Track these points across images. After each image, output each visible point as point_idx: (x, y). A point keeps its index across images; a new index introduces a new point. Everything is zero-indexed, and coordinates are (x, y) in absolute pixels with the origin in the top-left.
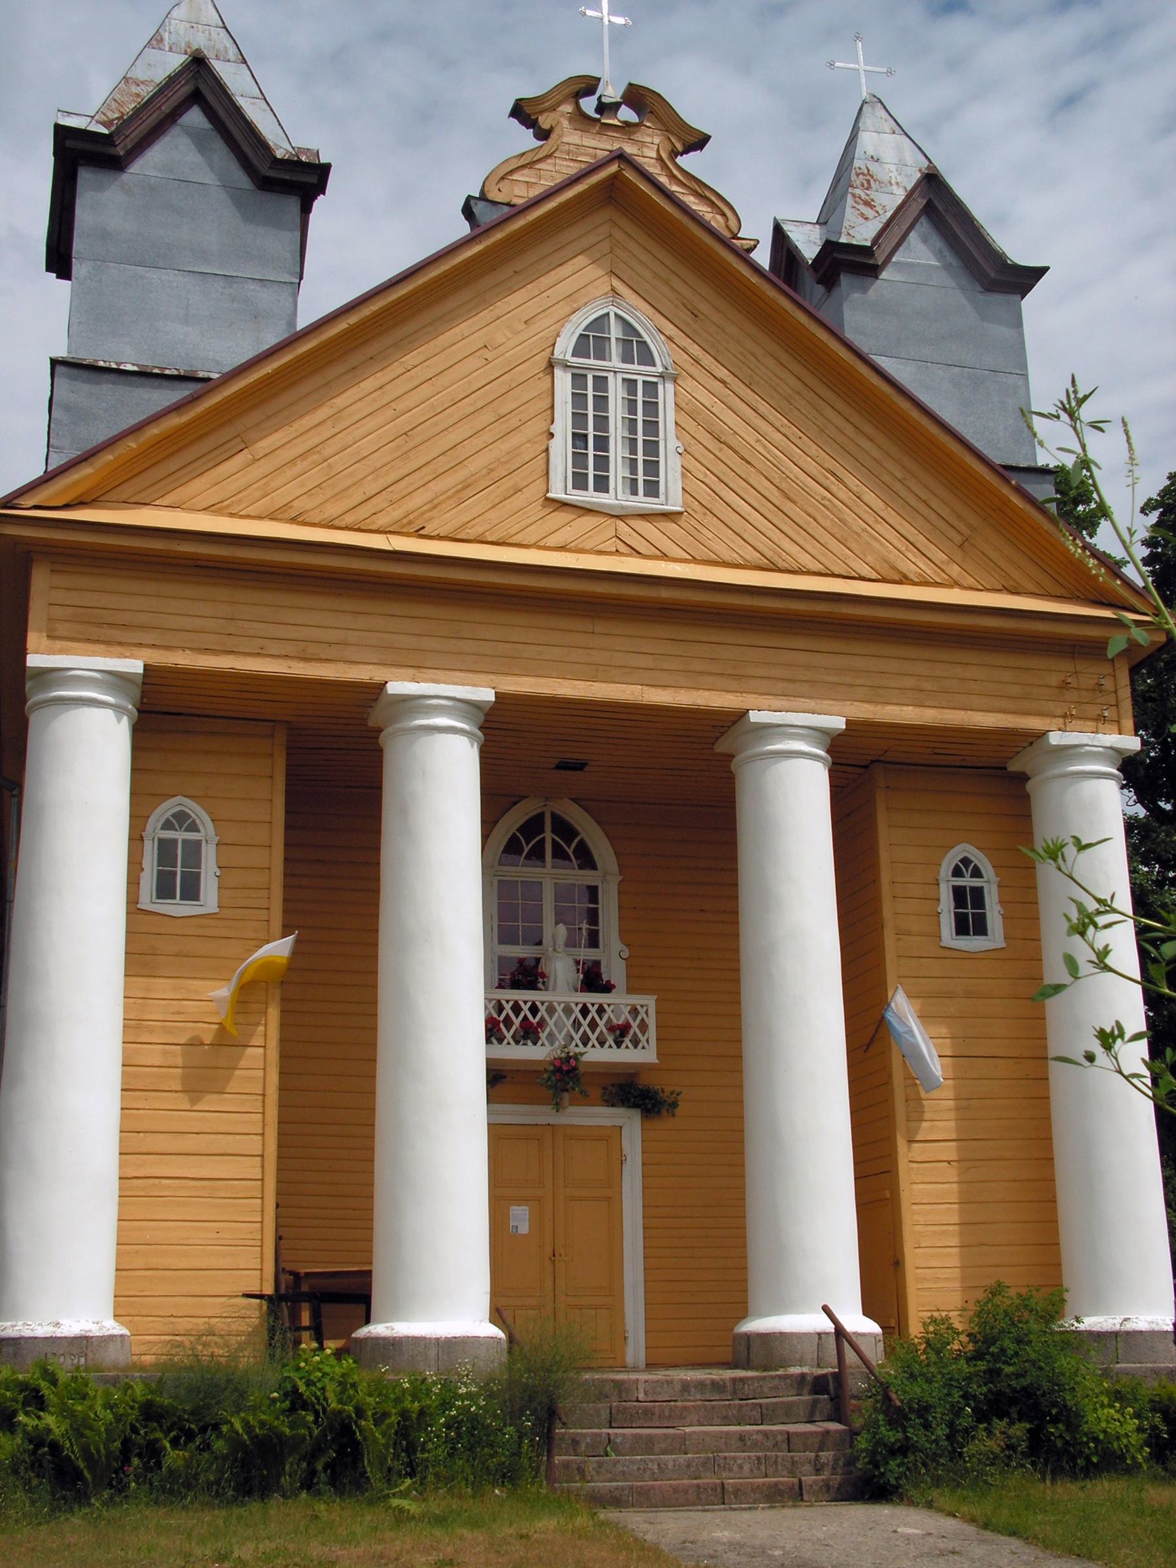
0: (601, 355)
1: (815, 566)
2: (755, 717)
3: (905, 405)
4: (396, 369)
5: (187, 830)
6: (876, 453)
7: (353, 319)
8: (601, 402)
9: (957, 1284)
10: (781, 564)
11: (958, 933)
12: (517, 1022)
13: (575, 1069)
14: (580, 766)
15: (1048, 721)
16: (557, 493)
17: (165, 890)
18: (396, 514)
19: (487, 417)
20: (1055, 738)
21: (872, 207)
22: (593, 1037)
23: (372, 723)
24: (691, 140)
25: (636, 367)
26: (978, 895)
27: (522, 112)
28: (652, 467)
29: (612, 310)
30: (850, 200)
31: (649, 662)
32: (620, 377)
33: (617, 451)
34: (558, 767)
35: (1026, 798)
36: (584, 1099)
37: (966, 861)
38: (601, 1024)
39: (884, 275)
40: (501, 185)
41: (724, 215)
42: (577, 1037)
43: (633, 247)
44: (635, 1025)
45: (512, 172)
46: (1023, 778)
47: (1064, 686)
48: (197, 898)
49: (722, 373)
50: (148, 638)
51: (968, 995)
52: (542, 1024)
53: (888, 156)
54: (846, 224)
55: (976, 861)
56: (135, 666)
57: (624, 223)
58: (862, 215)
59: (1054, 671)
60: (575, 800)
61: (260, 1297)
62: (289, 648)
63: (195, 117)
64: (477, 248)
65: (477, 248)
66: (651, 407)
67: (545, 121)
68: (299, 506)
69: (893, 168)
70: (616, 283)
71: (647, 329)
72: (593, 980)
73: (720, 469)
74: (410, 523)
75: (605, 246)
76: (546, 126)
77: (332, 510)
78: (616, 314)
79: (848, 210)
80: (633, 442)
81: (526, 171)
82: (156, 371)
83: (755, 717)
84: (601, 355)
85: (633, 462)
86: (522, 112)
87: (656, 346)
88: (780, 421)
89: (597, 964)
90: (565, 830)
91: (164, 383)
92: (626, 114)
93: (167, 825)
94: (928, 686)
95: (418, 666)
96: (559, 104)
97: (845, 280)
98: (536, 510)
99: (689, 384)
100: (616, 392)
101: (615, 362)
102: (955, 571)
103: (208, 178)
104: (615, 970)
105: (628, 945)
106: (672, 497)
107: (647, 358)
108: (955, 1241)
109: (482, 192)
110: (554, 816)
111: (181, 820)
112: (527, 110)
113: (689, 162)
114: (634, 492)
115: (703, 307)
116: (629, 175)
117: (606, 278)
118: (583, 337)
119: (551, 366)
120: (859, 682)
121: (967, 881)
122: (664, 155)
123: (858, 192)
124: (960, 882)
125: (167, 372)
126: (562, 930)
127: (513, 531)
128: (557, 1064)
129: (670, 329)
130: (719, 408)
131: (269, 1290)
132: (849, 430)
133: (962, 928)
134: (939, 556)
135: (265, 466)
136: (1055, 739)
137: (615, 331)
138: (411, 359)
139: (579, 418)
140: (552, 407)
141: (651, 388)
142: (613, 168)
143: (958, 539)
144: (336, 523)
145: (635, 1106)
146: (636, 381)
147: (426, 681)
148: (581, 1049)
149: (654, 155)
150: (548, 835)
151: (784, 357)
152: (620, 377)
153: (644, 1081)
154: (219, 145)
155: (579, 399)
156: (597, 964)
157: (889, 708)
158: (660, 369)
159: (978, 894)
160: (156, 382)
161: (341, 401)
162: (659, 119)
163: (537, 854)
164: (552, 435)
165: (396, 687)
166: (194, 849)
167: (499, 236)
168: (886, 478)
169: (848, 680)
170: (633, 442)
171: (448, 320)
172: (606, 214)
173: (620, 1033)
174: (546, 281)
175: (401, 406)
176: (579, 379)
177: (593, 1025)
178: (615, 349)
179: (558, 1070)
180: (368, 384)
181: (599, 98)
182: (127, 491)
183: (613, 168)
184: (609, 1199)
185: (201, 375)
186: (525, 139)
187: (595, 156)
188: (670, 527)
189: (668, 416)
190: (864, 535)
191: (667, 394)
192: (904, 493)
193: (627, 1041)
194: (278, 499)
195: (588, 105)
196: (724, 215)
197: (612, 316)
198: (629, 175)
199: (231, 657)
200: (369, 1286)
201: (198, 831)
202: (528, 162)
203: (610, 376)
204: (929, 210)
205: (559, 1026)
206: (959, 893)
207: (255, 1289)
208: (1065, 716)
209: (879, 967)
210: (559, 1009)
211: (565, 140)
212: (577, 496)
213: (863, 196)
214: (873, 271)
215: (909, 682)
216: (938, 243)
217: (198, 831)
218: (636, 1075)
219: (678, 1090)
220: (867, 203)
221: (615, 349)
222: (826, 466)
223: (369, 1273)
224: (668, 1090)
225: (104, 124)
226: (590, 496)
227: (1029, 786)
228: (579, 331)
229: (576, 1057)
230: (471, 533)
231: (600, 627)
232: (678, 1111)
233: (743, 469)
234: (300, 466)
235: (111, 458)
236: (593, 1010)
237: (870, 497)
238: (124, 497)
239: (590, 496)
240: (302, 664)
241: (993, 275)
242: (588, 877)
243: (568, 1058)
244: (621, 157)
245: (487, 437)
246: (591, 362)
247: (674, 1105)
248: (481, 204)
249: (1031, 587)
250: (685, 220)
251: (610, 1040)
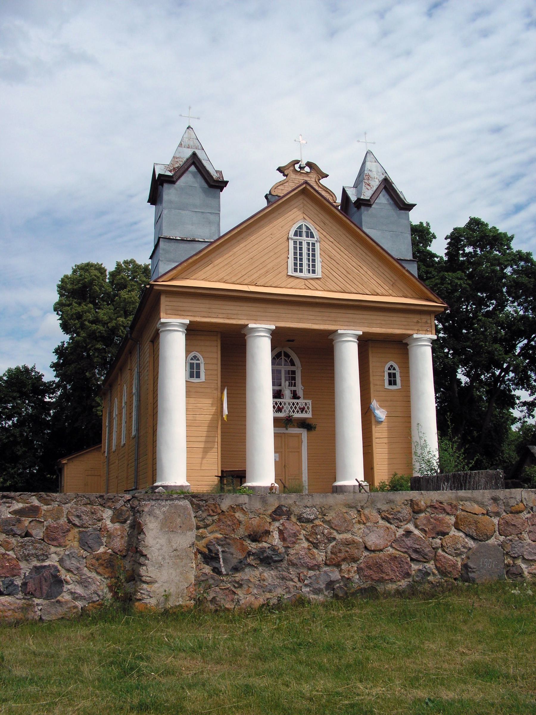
0: (301, 236)
1: (355, 291)
2: (339, 332)
3: (379, 248)
4: (249, 241)
5: (197, 360)
6: (371, 261)
7: (239, 229)
8: (301, 249)
9: (387, 474)
10: (347, 291)
11: (389, 385)
12: (276, 407)
13: (291, 419)
14: (293, 341)
15: (413, 331)
17: (192, 376)
18: (250, 280)
19: (271, 254)
20: (415, 336)
21: (370, 186)
22: (296, 411)
23: (242, 332)
24: (324, 176)
25: (309, 239)
27: (280, 170)
28: (314, 266)
29: (304, 223)
30: (364, 184)
31: (313, 317)
32: (306, 241)
33: (305, 262)
34: (287, 341)
35: (407, 349)
36: (294, 426)
37: (392, 366)
38: (298, 407)
39: (373, 206)
40: (275, 190)
41: (332, 196)
42: (291, 411)
43: (309, 206)
44: (306, 408)
45: (278, 186)
46: (407, 344)
47: (418, 322)
48: (200, 378)
49: (332, 240)
50: (190, 314)
51: (391, 401)
52: (283, 407)
53: (374, 169)
54: (363, 191)
55: (394, 366)
56: (187, 321)
57: (306, 199)
58: (367, 188)
59: (415, 318)
60: (290, 348)
61: (218, 476)
62: (224, 316)
63: (193, 168)
64: (270, 209)
65: (270, 209)
66: (314, 250)
67: (286, 173)
68: (226, 278)
69: (375, 173)
70: (305, 216)
71: (312, 229)
72: (295, 396)
73: (331, 266)
74: (253, 282)
75: (302, 206)
76: (286, 174)
77: (234, 279)
78: (305, 225)
79: (363, 187)
80: (309, 259)
81: (281, 186)
82: (185, 239)
83: (339, 332)
84: (301, 236)
85: (309, 265)
86: (280, 170)
87: (315, 233)
88: (347, 252)
89: (296, 391)
90: (287, 355)
91: (188, 242)
92: (307, 169)
93: (192, 359)
94: (383, 322)
95: (256, 320)
96: (290, 167)
97: (363, 208)
98: (285, 278)
99: (323, 243)
100: (305, 246)
101: (304, 237)
102: (391, 292)
103: (196, 185)
104: (300, 393)
105: (303, 386)
106: (319, 274)
107: (312, 236)
108: (386, 463)
109: (270, 192)
110: (285, 353)
111: (195, 357)
112: (281, 169)
113: (323, 181)
114: (309, 273)
115: (327, 222)
116: (308, 187)
117: (302, 214)
118: (296, 231)
119: (288, 239)
120: (365, 322)
121: (392, 371)
122: (317, 181)
123: (366, 181)
124: (390, 371)
125: (188, 239)
126: (287, 383)
127: (279, 284)
128: (287, 418)
129: (318, 228)
130: (331, 249)
131: (220, 475)
132: (364, 254)
133: (390, 383)
134: (387, 288)
135: (217, 268)
136: (415, 336)
137: (304, 229)
138: (252, 238)
139: (295, 253)
140: (289, 250)
141: (313, 244)
142: (304, 186)
143: (392, 283)
144: (235, 283)
145: (305, 428)
146: (309, 243)
147: (258, 324)
148: (293, 414)
149: (314, 180)
150: (283, 357)
151: (347, 235)
152: (306, 241)
153: (307, 422)
154: (199, 176)
155: (295, 248)
156: (296, 391)
157: (373, 328)
158: (316, 239)
159: (394, 375)
160: (185, 242)
161: (235, 250)
162: (315, 170)
164: (288, 258)
165: (251, 326)
166: (198, 365)
167: (275, 205)
168: (373, 267)
169: (363, 321)
170: (309, 259)
171: (262, 227)
172: (301, 197)
173: (302, 410)
174: (286, 215)
175: (250, 251)
176: (295, 243)
177: (296, 408)
178: (304, 234)
179: (287, 419)
180: (242, 245)
181: (300, 165)
182: (183, 275)
183: (304, 186)
184: (298, 452)
185: (197, 240)
186: (281, 177)
187: (299, 181)
188: (318, 281)
189: (318, 252)
190: (368, 283)
191: (317, 246)
192: (378, 271)
193: (304, 412)
194: (221, 276)
195: (297, 167)
196: (332, 196)
197: (304, 225)
198: (308, 187)
199: (210, 318)
200: (245, 474)
201: (199, 360)
202: (281, 183)
203: (303, 241)
204: (385, 188)
205: (287, 408)
206: (390, 374)
207: (217, 475)
208: (418, 330)
209: (369, 393)
210: (287, 403)
211: (291, 177)
212: (295, 274)
213: (367, 183)
214: (370, 206)
215: (378, 322)
216: (387, 197)
217: (199, 360)
218: (306, 420)
219: (316, 424)
220: (368, 185)
221: (304, 234)
222: (358, 264)
223: (245, 471)
224: (314, 424)
225: (170, 171)
226: (298, 274)
227: (408, 347)
228: (295, 229)
229: (292, 416)
230: (269, 285)
231: (301, 308)
232: (316, 429)
233: (337, 266)
234: (226, 268)
235: (180, 268)
236: (296, 404)
237: (369, 272)
238: (182, 277)
239: (298, 274)
240: (228, 320)
241: (402, 206)
242: (292, 368)
243: (289, 417)
244: (306, 183)
245: (272, 259)
246: (298, 237)
247: (315, 428)
248: (270, 196)
249: (410, 296)
250: (323, 200)
251: (300, 412)
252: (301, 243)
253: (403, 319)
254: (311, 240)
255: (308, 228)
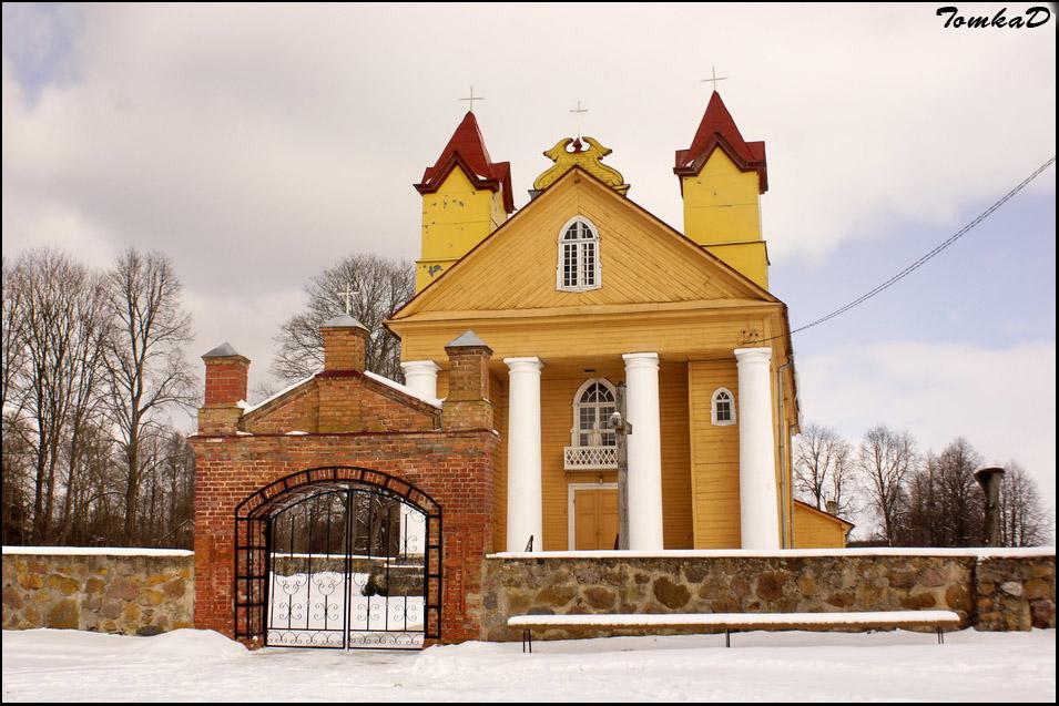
16: (559, 288)
18: (508, 302)
26: (727, 405)
28: (591, 274)
37: (723, 394)
84: (575, 237)
87: (594, 232)
90: (602, 387)
107: (590, 235)
113: (606, 161)
118: (568, 232)
121: (723, 401)
133: (720, 417)
139: (567, 262)
141: (591, 246)
142: (574, 171)
150: (597, 391)
155: (567, 255)
163: (593, 399)
176: (567, 248)
178: (579, 234)
186: (549, 164)
198: (580, 172)
202: (548, 173)
206: (719, 405)
227: (738, 365)
239: (571, 287)
252: (574, 247)
253: (718, 330)
254: (588, 241)
255: (585, 226)
